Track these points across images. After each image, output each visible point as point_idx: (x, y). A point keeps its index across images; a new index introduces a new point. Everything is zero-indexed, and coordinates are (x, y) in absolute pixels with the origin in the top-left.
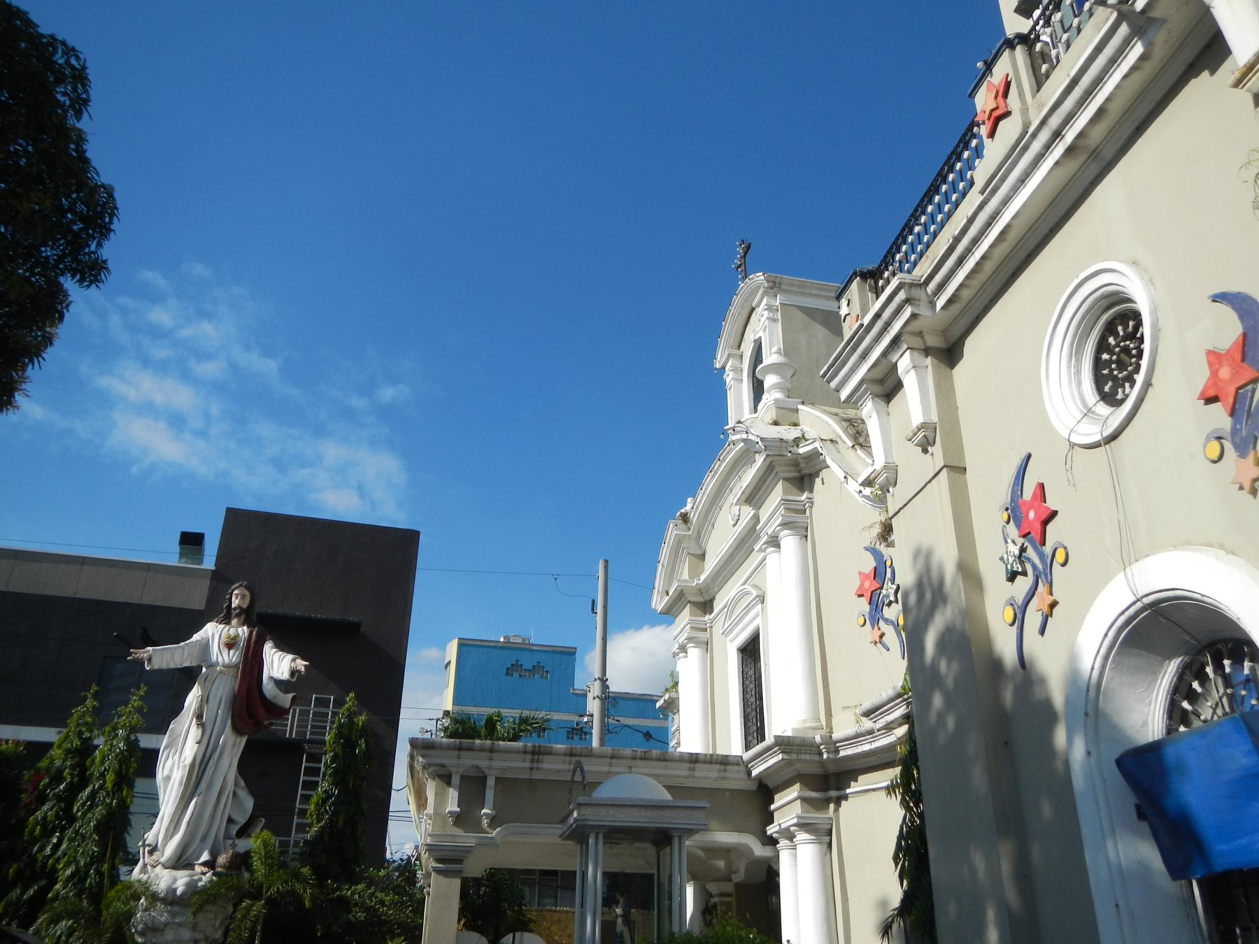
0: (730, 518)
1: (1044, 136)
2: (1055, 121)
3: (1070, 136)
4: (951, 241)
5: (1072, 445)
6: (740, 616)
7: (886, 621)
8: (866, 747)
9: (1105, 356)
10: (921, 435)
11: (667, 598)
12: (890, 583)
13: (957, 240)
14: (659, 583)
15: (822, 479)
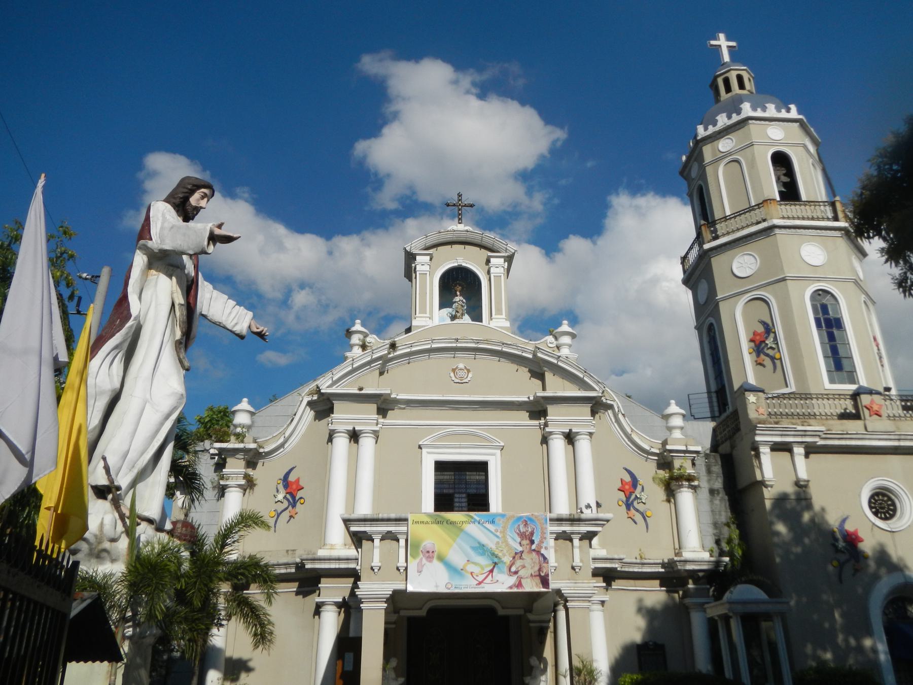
0: (452, 375)
1: (897, 437)
2: (903, 437)
3: (902, 443)
4: (845, 432)
5: (874, 524)
6: (461, 446)
7: (637, 510)
8: (636, 570)
9: (873, 501)
10: (806, 483)
11: (358, 392)
12: (642, 493)
13: (847, 434)
14: (339, 372)
15: (600, 417)
